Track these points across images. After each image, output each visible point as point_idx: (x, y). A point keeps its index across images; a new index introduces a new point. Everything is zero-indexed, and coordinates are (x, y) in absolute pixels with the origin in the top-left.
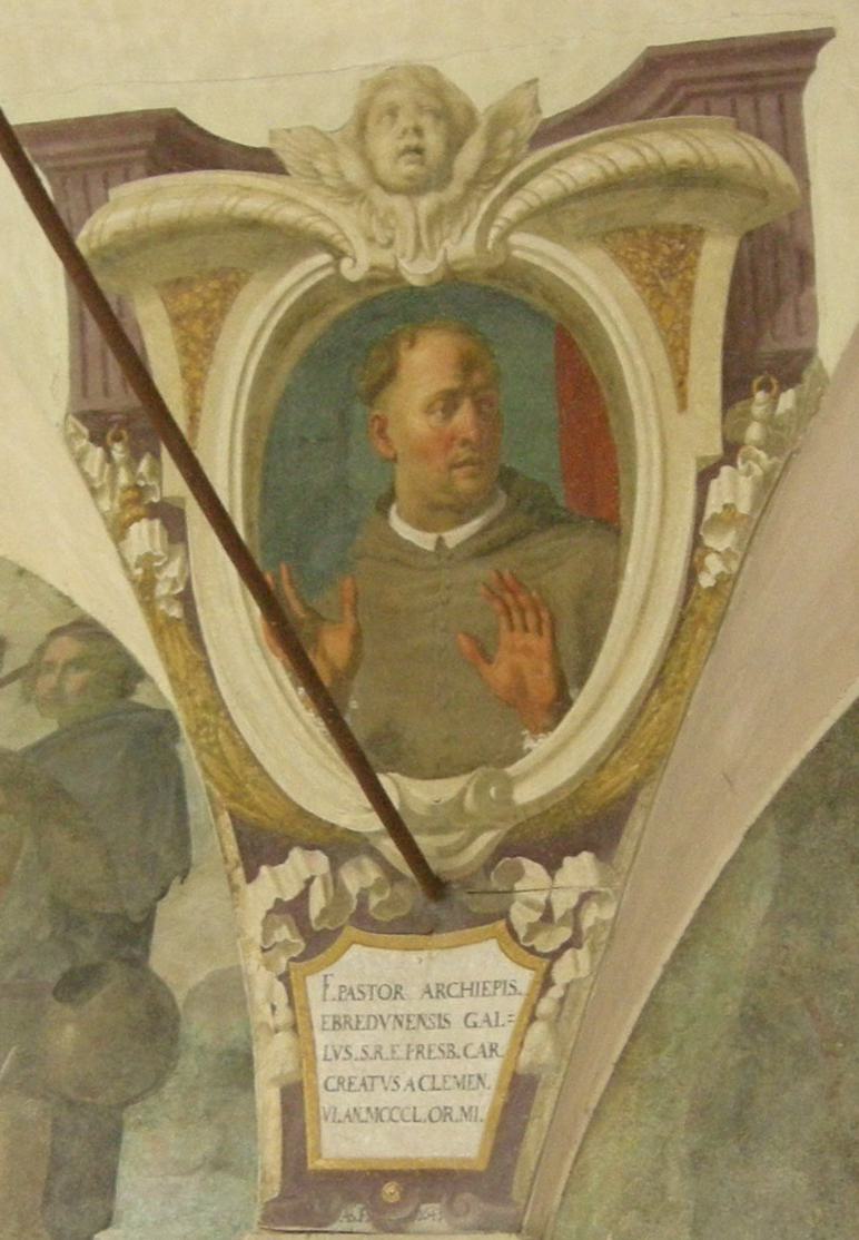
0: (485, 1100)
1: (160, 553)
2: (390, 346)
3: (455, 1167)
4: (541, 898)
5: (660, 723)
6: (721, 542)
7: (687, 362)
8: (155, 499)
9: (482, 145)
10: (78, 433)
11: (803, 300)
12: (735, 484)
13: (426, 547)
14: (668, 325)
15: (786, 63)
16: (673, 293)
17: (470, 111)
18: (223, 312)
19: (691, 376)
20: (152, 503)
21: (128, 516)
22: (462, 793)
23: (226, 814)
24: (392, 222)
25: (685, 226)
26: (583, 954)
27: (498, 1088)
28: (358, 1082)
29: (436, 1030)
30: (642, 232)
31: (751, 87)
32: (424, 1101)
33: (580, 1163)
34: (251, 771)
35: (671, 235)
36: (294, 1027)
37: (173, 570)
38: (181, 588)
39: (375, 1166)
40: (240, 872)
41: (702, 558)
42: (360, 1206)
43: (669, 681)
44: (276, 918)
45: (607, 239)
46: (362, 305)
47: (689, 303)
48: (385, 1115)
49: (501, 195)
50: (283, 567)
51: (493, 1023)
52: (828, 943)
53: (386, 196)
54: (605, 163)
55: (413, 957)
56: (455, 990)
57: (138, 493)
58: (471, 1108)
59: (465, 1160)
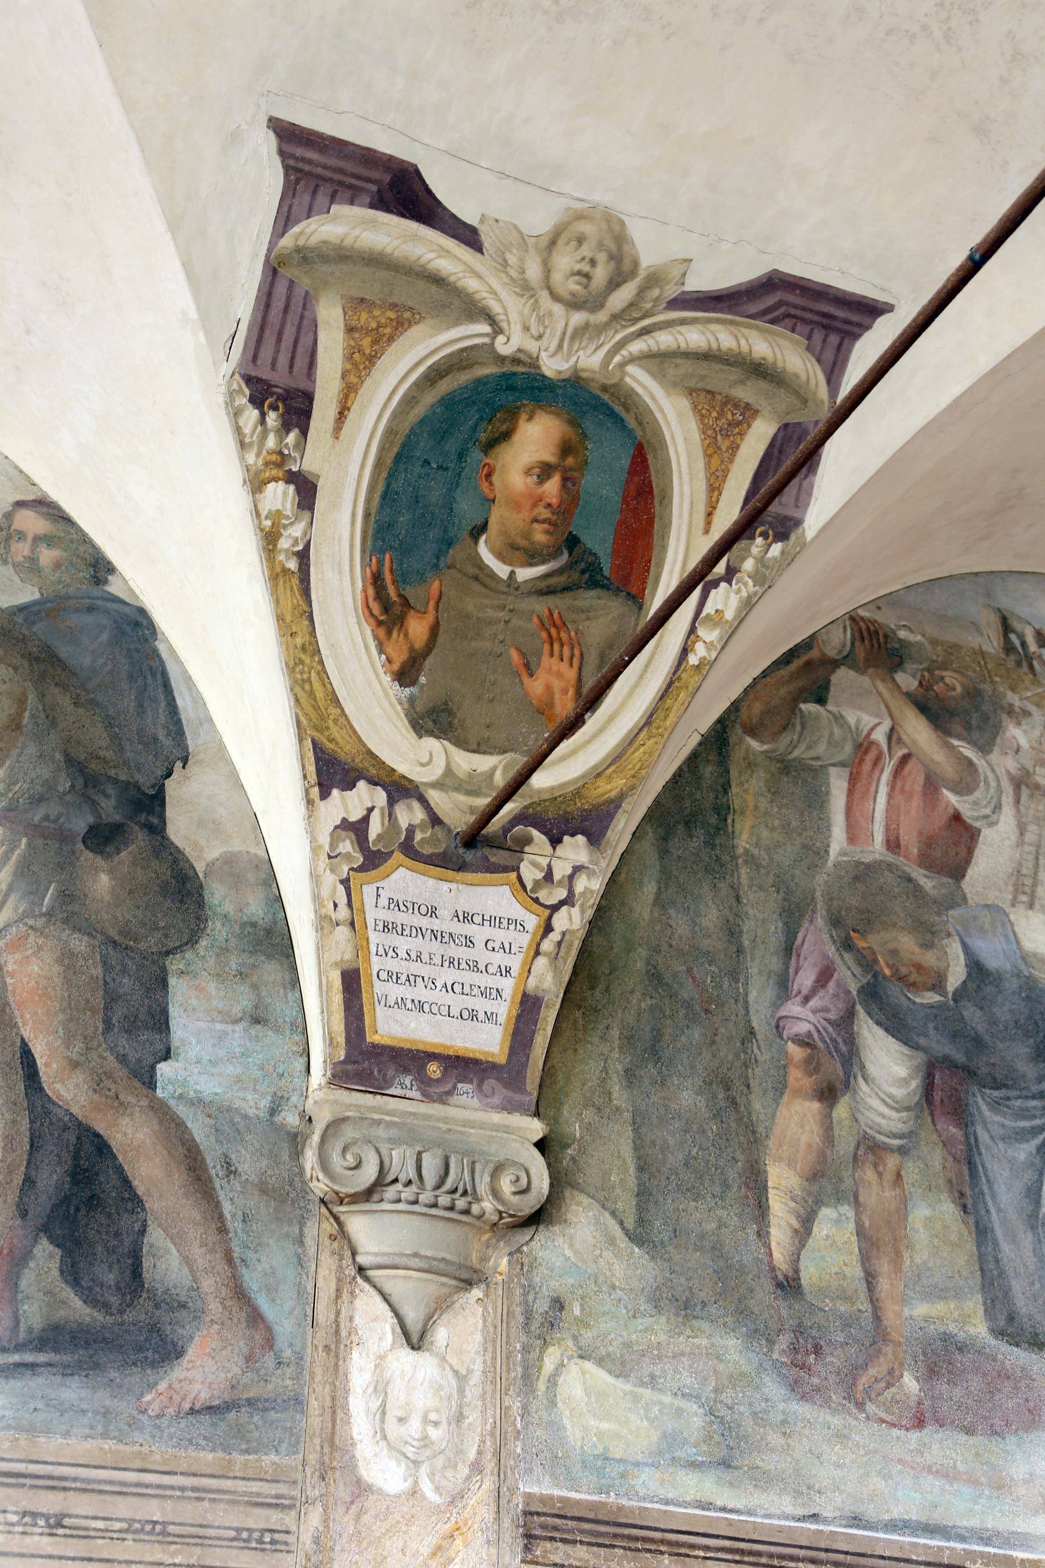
0: (504, 1009)
1: (289, 513)
2: (513, 415)
3: (482, 1057)
4: (544, 862)
5: (645, 753)
6: (708, 635)
7: (718, 501)
8: (295, 469)
9: (635, 292)
10: (240, 391)
11: (805, 483)
12: (727, 598)
13: (501, 575)
14: (713, 469)
15: (855, 318)
16: (724, 448)
17: (636, 263)
18: (391, 339)
19: (718, 510)
20: (290, 472)
21: (267, 474)
22: (494, 769)
24: (547, 322)
25: (747, 404)
26: (576, 911)
27: (512, 1002)
28: (403, 978)
29: (463, 948)
30: (718, 397)
31: (827, 324)
32: (457, 1002)
33: (549, 1064)
34: (334, 711)
35: (736, 406)
36: (352, 924)
37: (297, 530)
38: (300, 547)
39: (421, 1048)
41: (694, 643)
42: (411, 1077)
43: (655, 725)
44: (343, 834)
45: (694, 394)
46: (503, 375)
47: (731, 460)
48: (426, 1007)
49: (632, 333)
50: (387, 557)
51: (507, 951)
52: (697, 929)
53: (550, 300)
54: (712, 339)
55: (445, 886)
56: (478, 919)
57: (281, 458)
58: (492, 1014)
59: (488, 1053)
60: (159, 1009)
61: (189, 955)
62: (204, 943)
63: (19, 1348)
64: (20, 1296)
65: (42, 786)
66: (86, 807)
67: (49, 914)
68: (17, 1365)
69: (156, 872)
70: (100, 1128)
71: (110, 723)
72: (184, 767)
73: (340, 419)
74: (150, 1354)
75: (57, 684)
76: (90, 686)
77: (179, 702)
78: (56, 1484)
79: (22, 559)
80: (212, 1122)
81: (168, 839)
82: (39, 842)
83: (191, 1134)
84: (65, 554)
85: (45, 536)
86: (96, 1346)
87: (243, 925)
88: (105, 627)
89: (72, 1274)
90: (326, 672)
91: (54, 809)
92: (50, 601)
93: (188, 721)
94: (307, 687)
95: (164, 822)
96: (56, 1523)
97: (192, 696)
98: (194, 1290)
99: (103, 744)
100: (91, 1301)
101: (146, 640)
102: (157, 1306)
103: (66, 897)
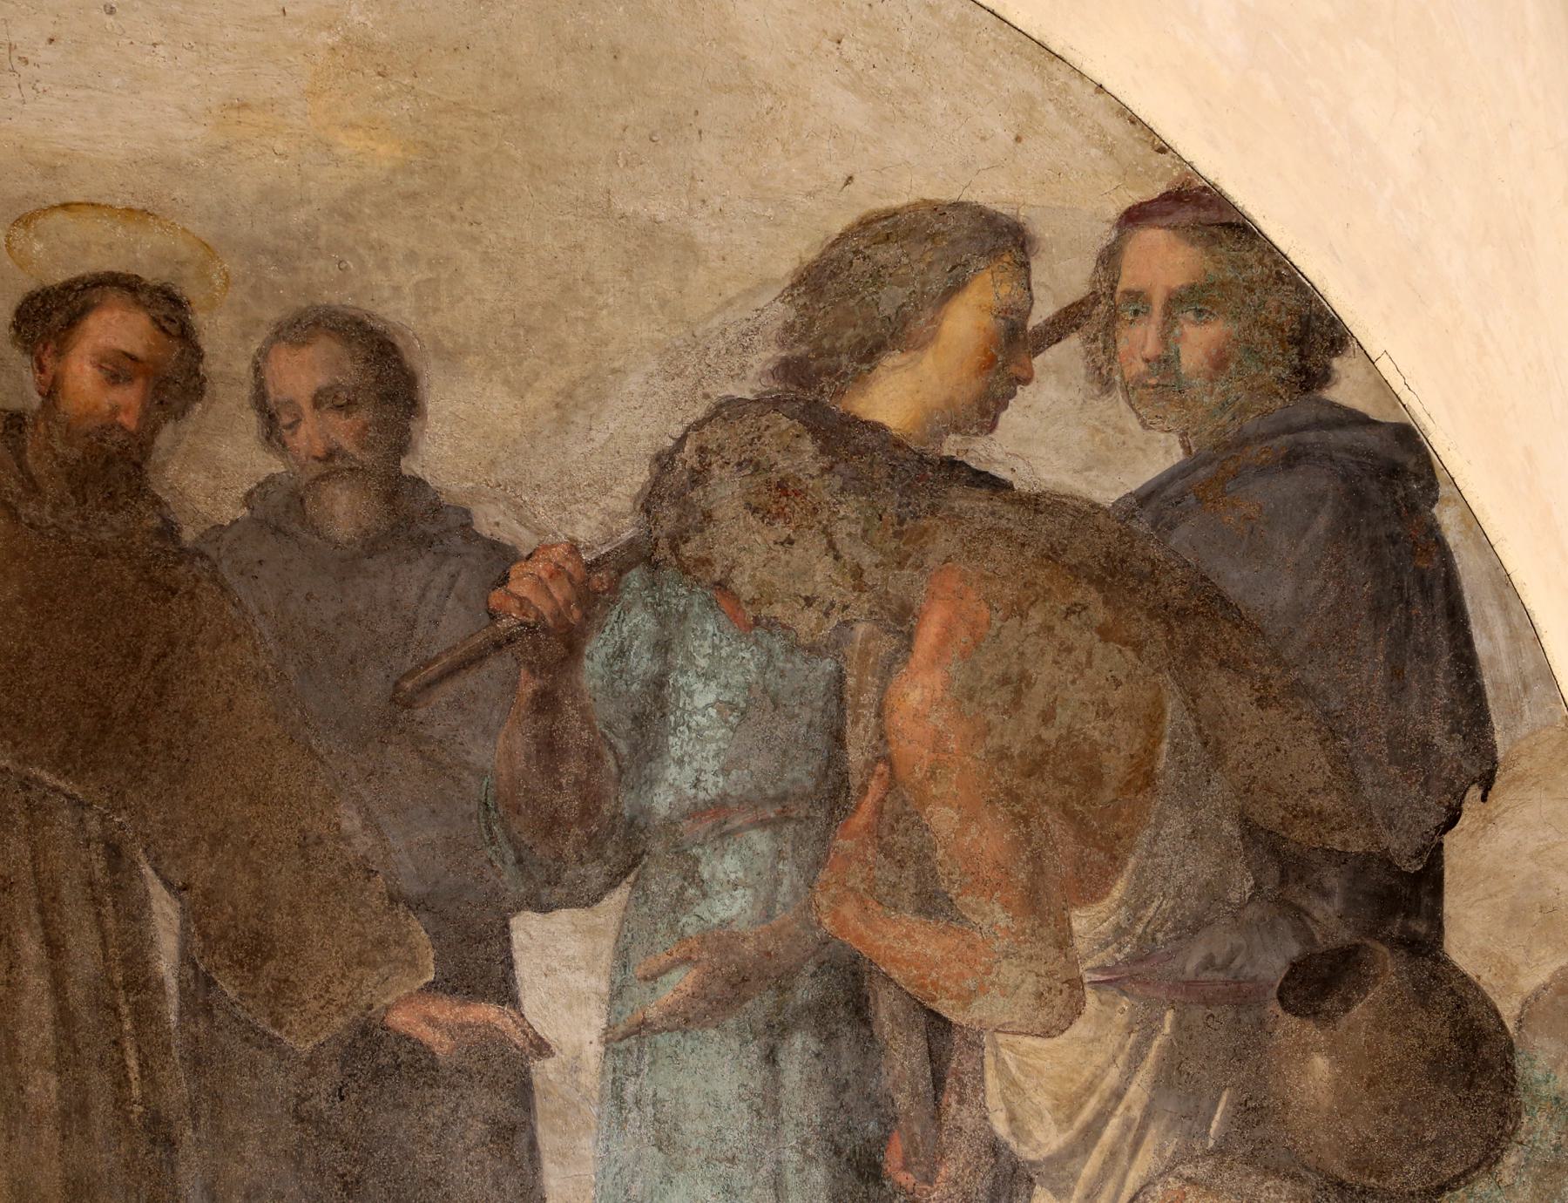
62: (1511, 1159)
65: (1199, 898)
66: (1284, 926)
67: (1221, 1151)
69: (1421, 1035)
71: (1331, 729)
72: (1484, 799)
75: (1222, 664)
76: (1289, 654)
77: (1481, 646)
79: (1143, 367)
81: (1447, 962)
82: (1197, 1013)
84: (1234, 328)
85: (1192, 288)
88: (1322, 498)
91: (1219, 941)
92: (1206, 462)
93: (1497, 686)
95: (1440, 927)
97: (1509, 624)
99: (1318, 780)
101: (1413, 509)
103: (1250, 1112)
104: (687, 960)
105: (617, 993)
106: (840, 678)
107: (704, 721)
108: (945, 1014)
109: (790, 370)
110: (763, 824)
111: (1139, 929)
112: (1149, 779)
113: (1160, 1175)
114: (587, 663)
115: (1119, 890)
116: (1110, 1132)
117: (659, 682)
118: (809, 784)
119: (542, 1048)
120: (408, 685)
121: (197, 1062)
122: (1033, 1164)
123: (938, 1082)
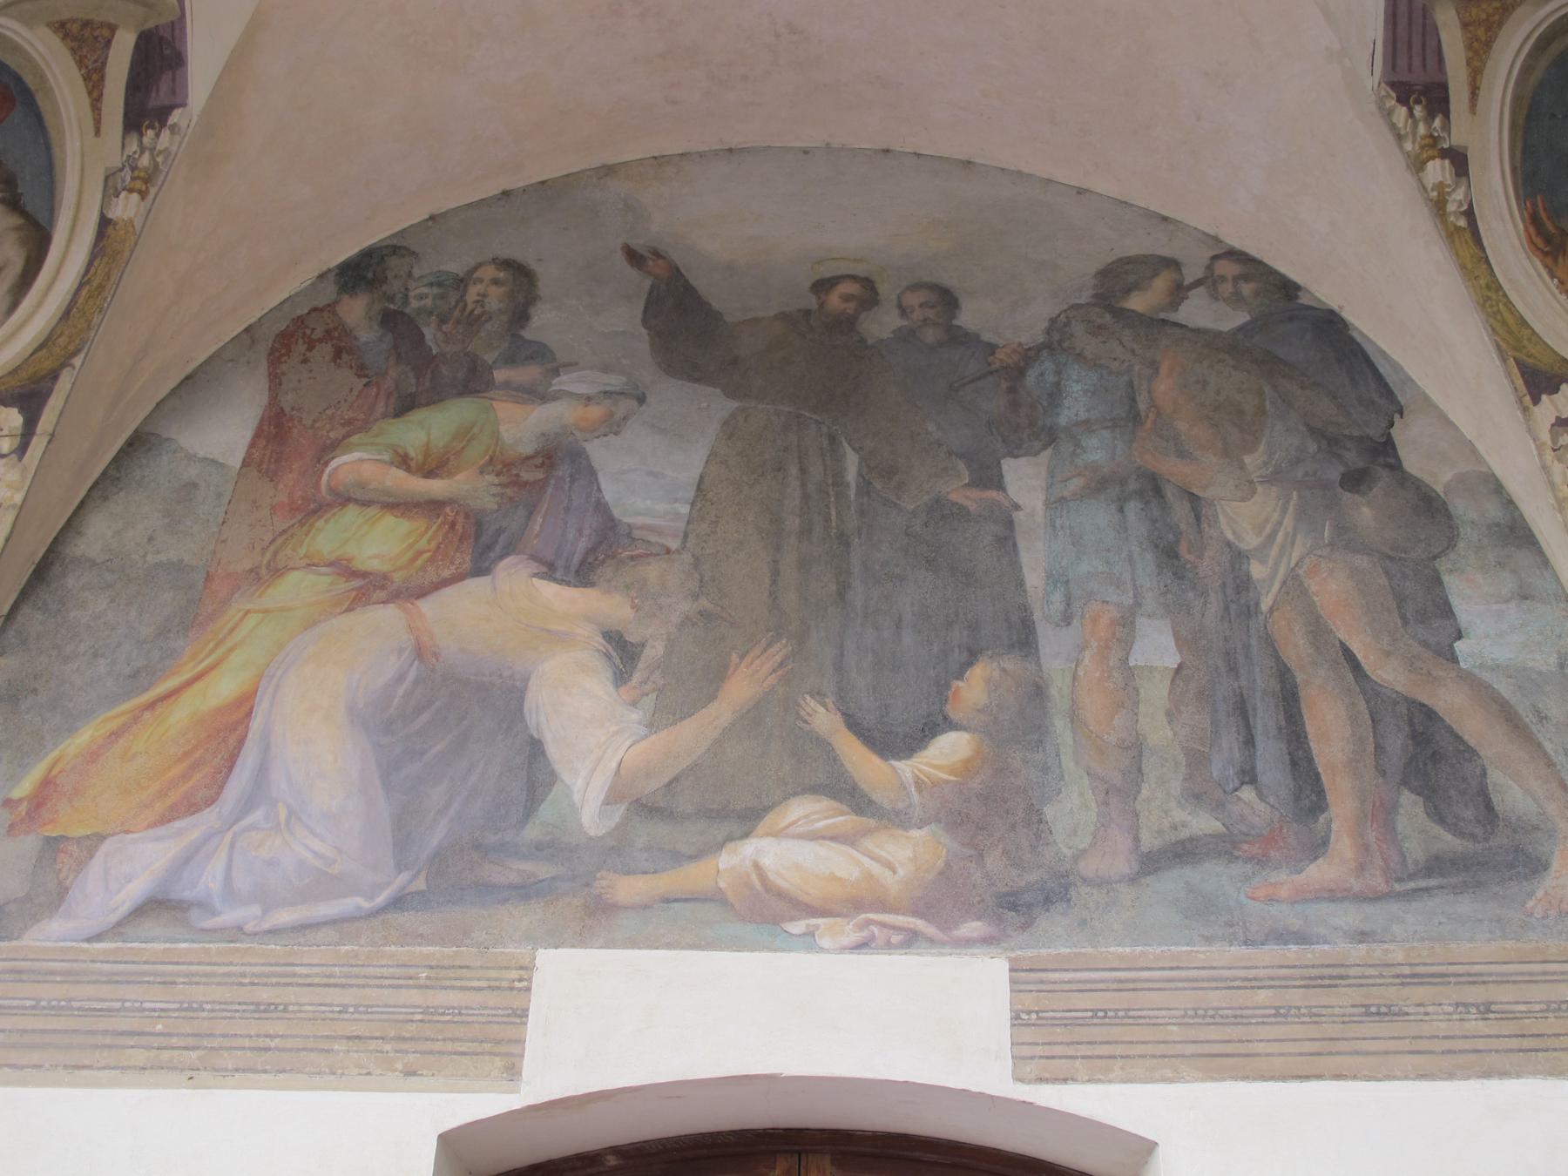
1: (1449, 182)
8: (1446, 146)
10: (1388, 96)
18: (1501, 24)
20: (1442, 150)
21: (1425, 156)
23: (1512, 359)
34: (1526, 332)
37: (1459, 195)
38: (1465, 207)
40: (1527, 399)
44: (1560, 429)
50: (1539, 198)
57: (1433, 141)
60: (1441, 601)
61: (1452, 556)
62: (1461, 545)
63: (1412, 877)
64: (1400, 837)
67: (1331, 544)
68: (1415, 890)
70: (1424, 699)
72: (1402, 417)
73: (1473, 97)
74: (1520, 869)
77: (1382, 370)
78: (1476, 980)
80: (1513, 681)
83: (1499, 693)
86: (1474, 869)
87: (1489, 527)
89: (1438, 815)
90: (1511, 303)
94: (1499, 317)
96: (1486, 1010)
98: (1541, 815)
100: (1459, 833)
102: (1515, 831)
103: (1341, 529)
104: (1079, 474)
105: (1049, 487)
106: (1131, 384)
107: (1077, 395)
108: (1195, 493)
109: (1096, 296)
110: (1107, 428)
111: (1274, 462)
112: (1264, 413)
113: (1308, 554)
114: (1028, 378)
115: (1262, 448)
116: (1280, 537)
117: (1058, 384)
118: (1124, 415)
119: (1017, 507)
120: (956, 385)
121: (862, 513)
122: (1247, 550)
123: (1198, 518)
